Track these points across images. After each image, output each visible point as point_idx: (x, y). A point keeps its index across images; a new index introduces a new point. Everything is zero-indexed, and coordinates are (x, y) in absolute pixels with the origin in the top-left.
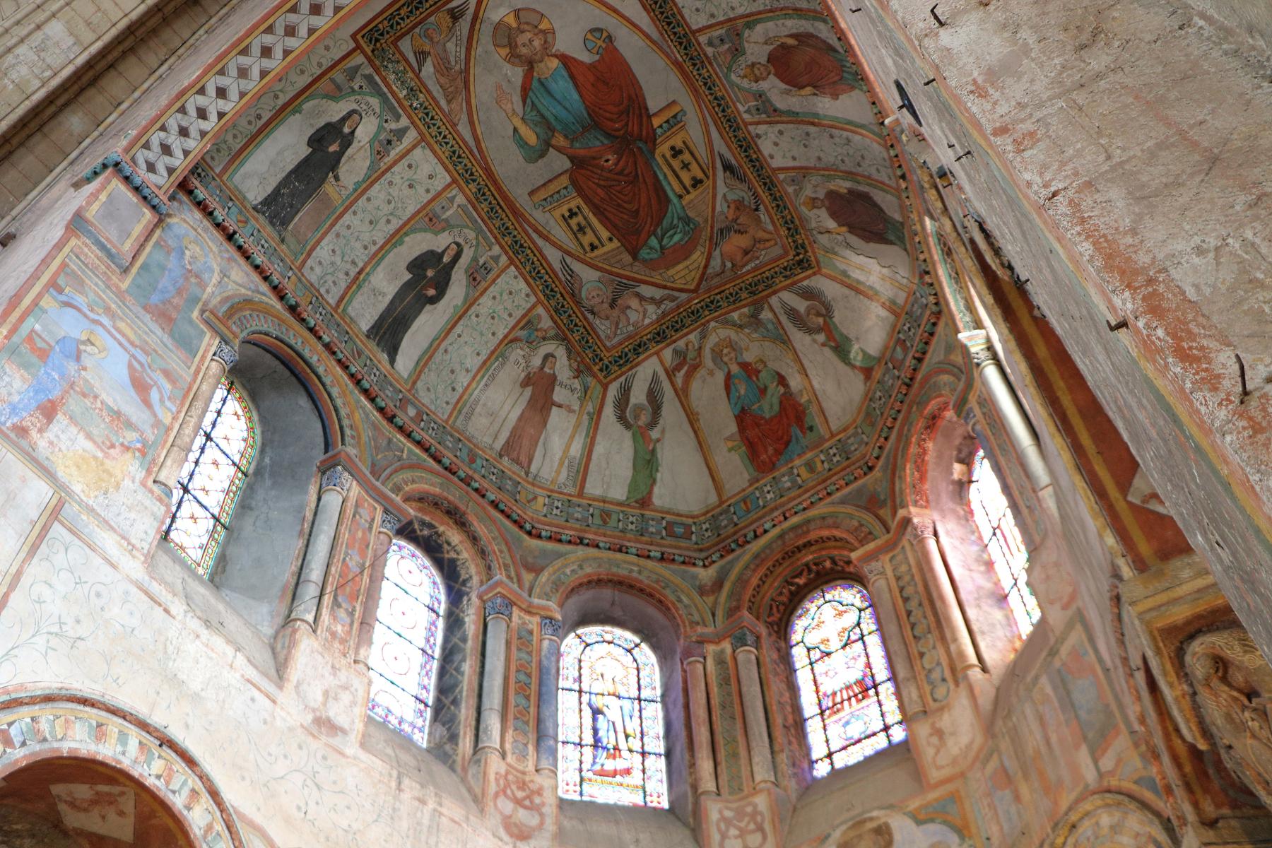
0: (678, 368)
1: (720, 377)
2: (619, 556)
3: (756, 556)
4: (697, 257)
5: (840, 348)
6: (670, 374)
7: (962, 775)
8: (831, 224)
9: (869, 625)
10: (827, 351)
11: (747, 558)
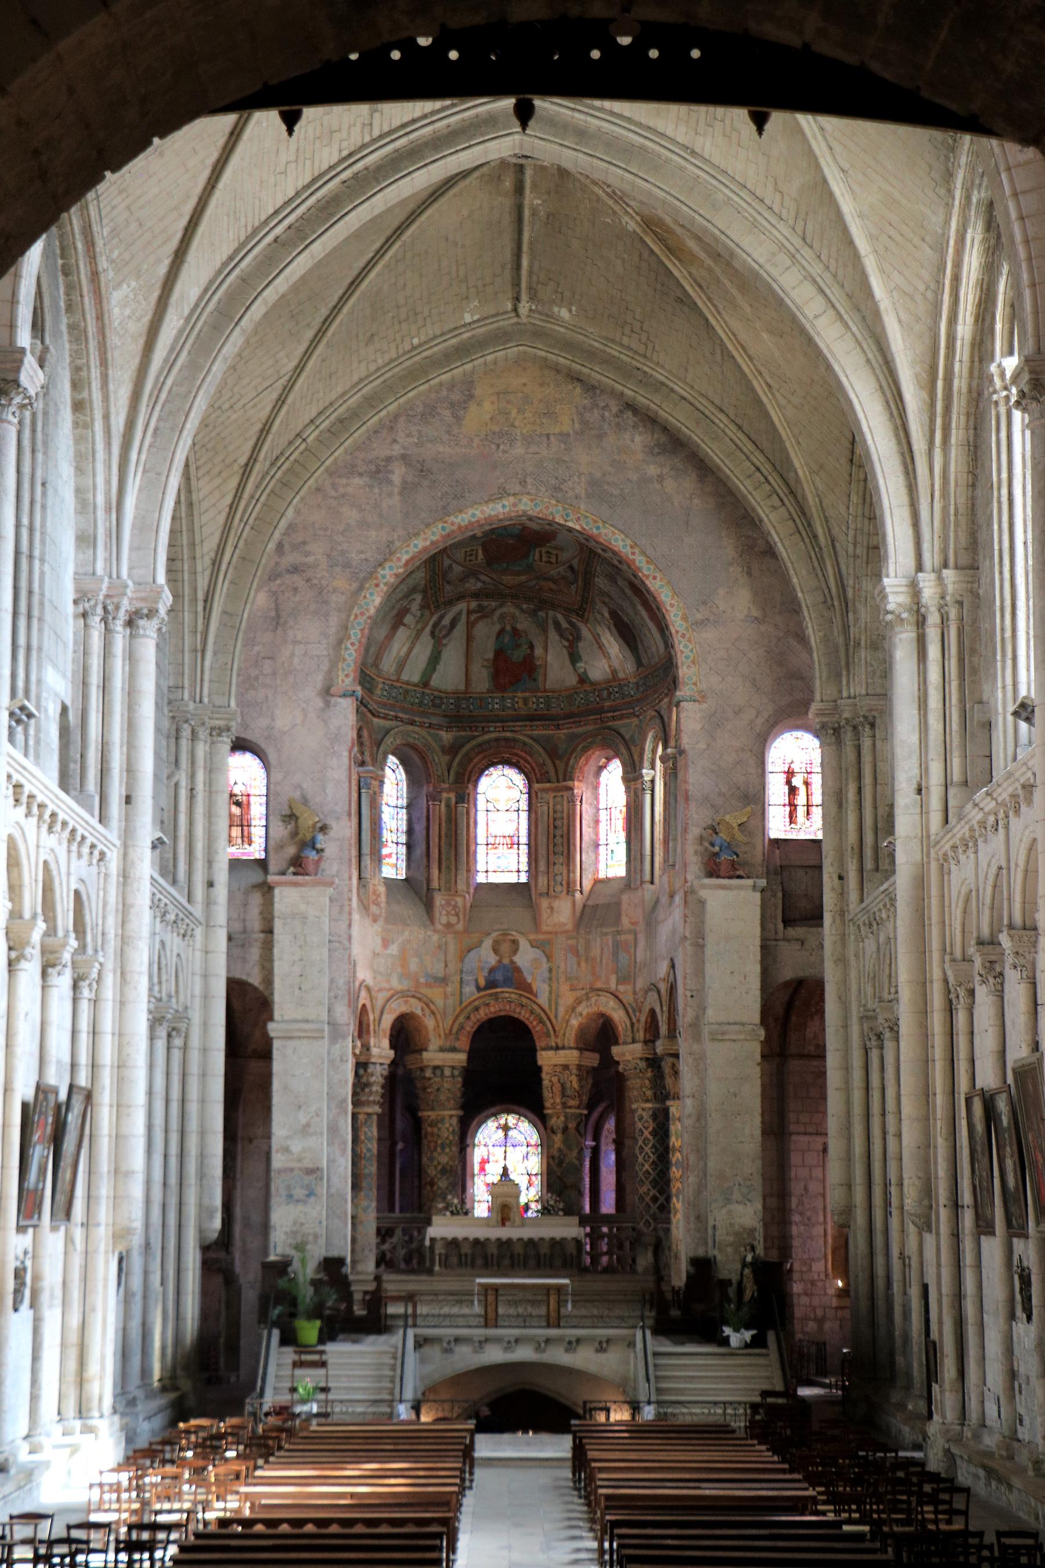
0: (475, 612)
1: (497, 627)
2: (411, 728)
3: (480, 745)
4: (523, 578)
5: (574, 657)
6: (469, 612)
7: (556, 933)
8: (607, 615)
9: (524, 805)
10: (565, 652)
11: (474, 743)
